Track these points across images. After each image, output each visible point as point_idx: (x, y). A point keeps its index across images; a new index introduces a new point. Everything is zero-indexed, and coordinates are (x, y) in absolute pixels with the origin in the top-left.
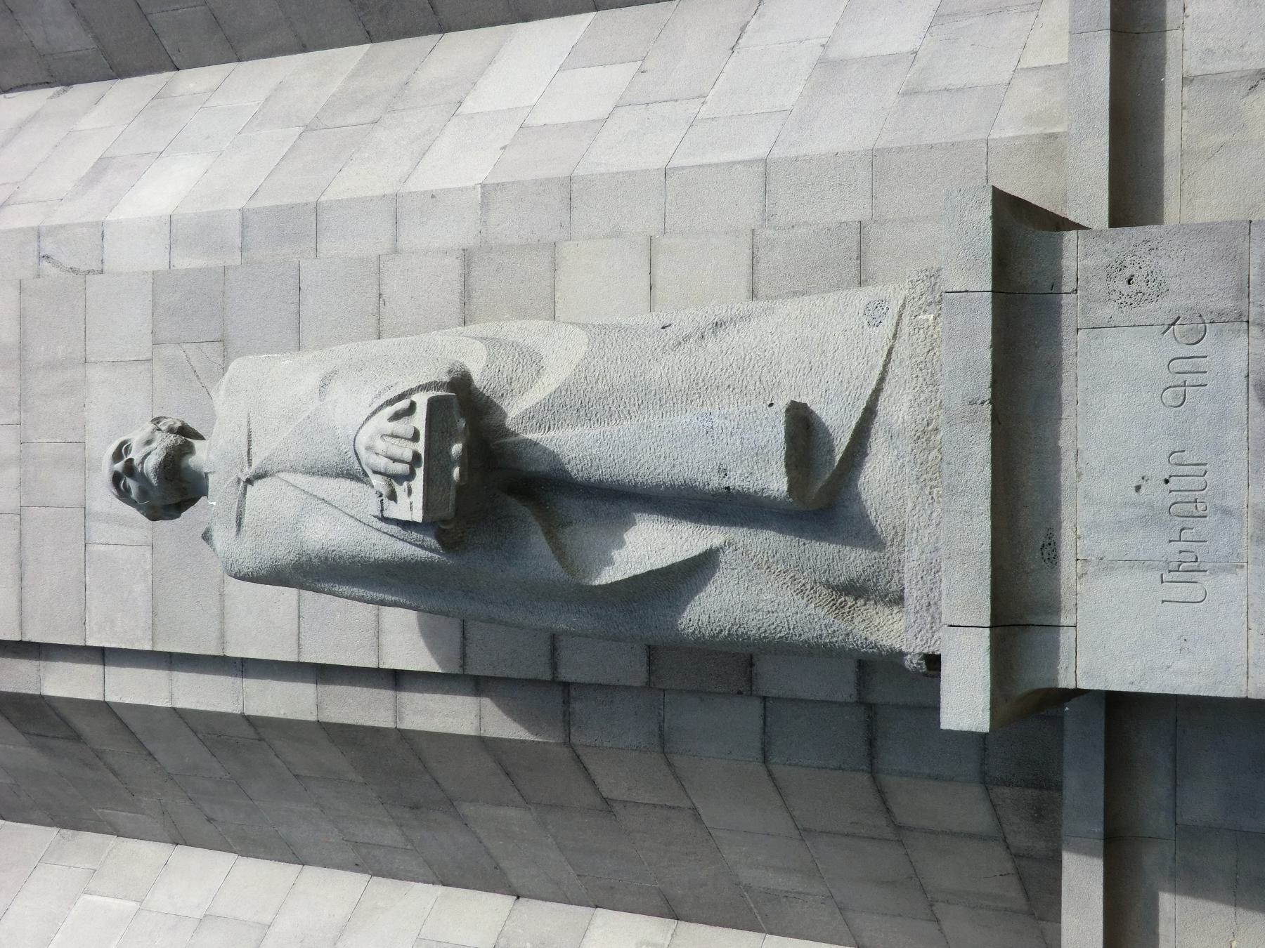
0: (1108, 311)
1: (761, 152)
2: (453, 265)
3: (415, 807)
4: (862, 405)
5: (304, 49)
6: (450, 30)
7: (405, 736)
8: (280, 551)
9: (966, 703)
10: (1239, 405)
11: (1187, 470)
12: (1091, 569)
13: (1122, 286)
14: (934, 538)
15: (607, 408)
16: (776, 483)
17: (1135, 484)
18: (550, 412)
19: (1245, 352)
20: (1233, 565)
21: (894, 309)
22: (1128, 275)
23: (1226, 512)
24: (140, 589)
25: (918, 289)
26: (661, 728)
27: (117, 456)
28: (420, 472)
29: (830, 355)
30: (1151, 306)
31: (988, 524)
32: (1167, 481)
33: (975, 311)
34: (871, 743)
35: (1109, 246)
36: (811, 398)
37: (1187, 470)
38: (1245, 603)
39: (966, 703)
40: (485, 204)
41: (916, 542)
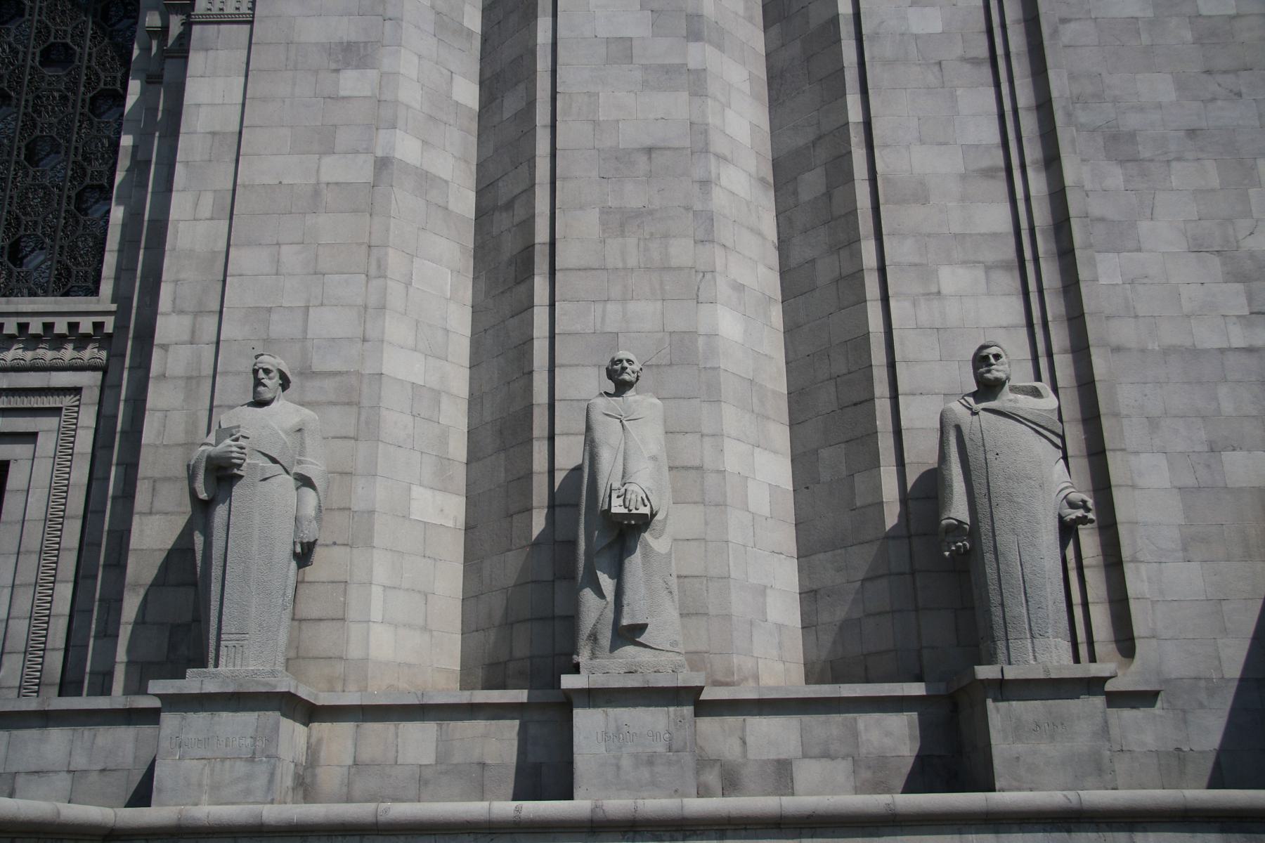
1: (733, 576)
2: (697, 463)
5: (787, 363)
7: (530, 440)
8: (599, 434)
9: (569, 682)
16: (625, 622)
18: (647, 545)
24: (578, 327)
27: (628, 361)
28: (626, 511)
34: (541, 619)
39: (569, 682)
40: (718, 472)
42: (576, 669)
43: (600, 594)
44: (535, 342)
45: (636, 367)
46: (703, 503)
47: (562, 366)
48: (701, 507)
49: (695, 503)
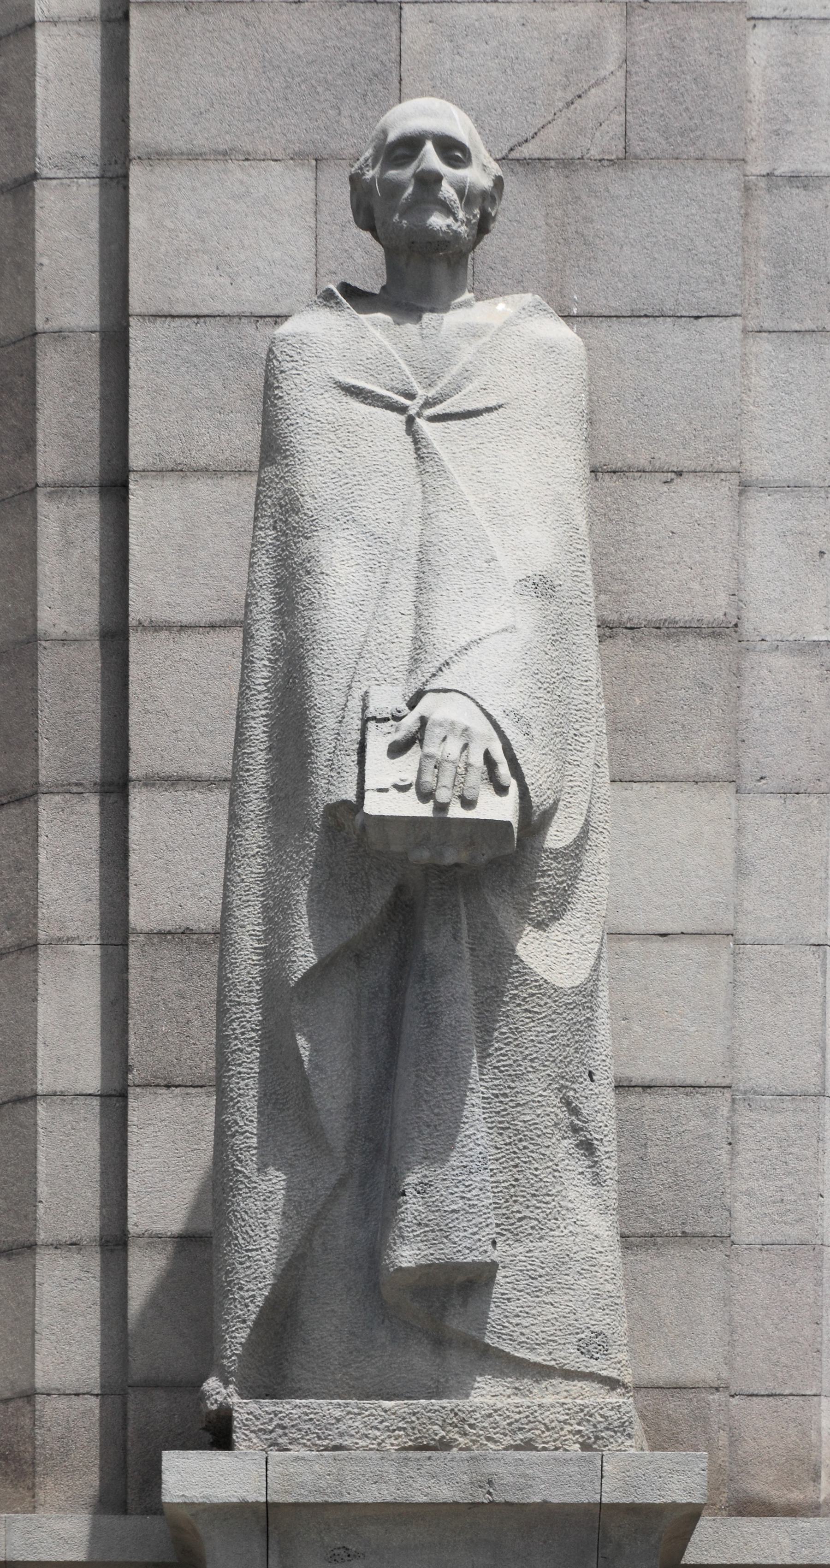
9: (190, 1477)
14: (353, 1432)
21: (595, 1366)
25: (612, 1413)
29: (548, 1299)
33: (582, 1486)
36: (502, 1281)
41: (349, 1413)
42: (219, 1434)
44: (42, 38)
45: (477, 176)
46: (733, 780)
47: (158, 156)
48: (726, 796)
49: (699, 780)
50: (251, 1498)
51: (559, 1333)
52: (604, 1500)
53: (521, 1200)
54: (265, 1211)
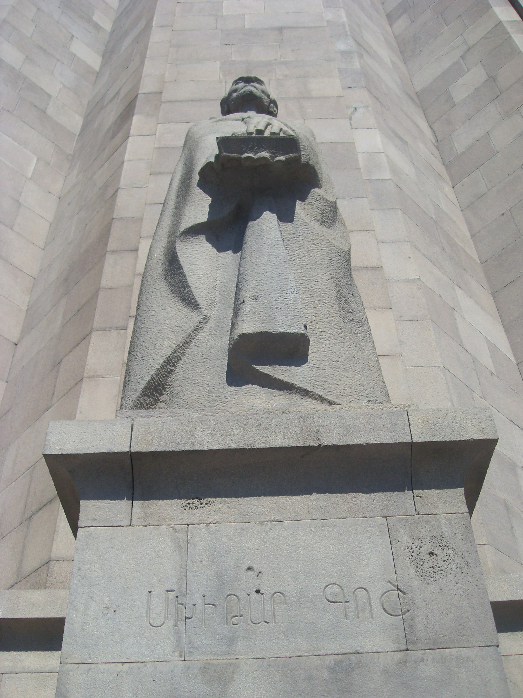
0: (405, 540)
3: (66, 280)
4: (309, 388)
6: (494, 297)
10: (332, 647)
11: (268, 607)
12: (179, 535)
13: (427, 547)
15: (297, 249)
16: (248, 326)
17: (255, 566)
19: (380, 650)
20: (182, 649)
22: (436, 552)
23: (232, 641)
26: (98, 376)
30: (412, 571)
31: (217, 447)
32: (258, 592)
35: (459, 536)
37: (268, 607)
38: (148, 659)
43: (189, 300)
50: (116, 449)
51: (354, 393)
52: (414, 441)
53: (321, 323)
54: (155, 339)
